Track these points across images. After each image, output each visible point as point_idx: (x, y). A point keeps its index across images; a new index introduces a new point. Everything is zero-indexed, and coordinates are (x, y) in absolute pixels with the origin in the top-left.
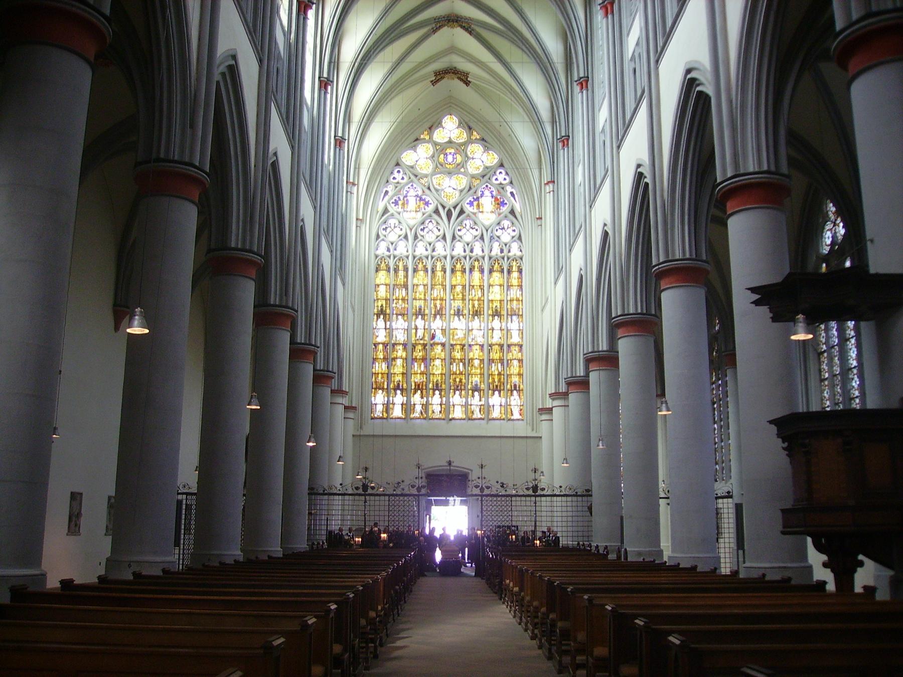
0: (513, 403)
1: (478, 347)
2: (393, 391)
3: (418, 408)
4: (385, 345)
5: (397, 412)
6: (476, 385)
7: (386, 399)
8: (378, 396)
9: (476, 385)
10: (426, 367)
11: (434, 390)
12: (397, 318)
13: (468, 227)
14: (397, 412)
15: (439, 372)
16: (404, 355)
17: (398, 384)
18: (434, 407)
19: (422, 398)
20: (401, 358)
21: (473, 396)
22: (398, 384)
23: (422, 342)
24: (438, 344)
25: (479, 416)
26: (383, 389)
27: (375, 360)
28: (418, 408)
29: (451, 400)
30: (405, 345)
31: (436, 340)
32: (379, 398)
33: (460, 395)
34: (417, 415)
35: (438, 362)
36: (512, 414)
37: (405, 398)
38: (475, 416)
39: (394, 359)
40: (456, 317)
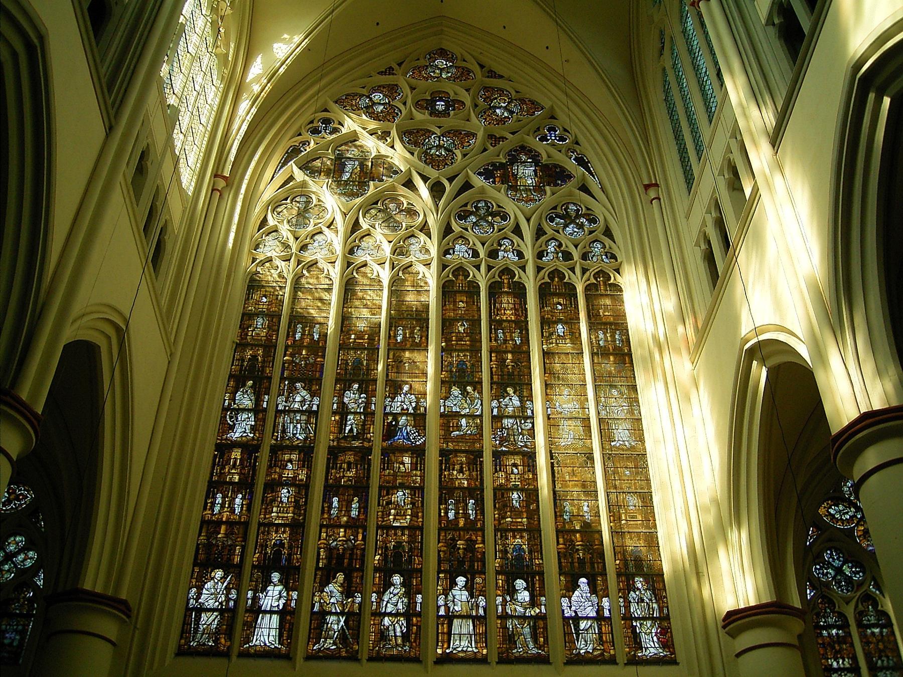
0: (636, 610)
1: (518, 460)
2: (257, 574)
3: (335, 624)
4: (249, 448)
5: (267, 633)
6: (519, 558)
7: (233, 595)
8: (209, 585)
9: (519, 558)
10: (364, 507)
11: (386, 573)
12: (292, 390)
13: (482, 212)
14: (267, 633)
15: (405, 522)
16: (302, 476)
17: (278, 554)
18: (387, 621)
19: (348, 592)
20: (293, 483)
21: (512, 591)
22: (278, 554)
23: (356, 444)
24: (403, 450)
25: (535, 651)
26: (227, 568)
27: (215, 486)
28: (335, 624)
29: (441, 602)
30: (306, 452)
31: (399, 440)
32: (213, 591)
33: (469, 587)
34: (329, 644)
35: (399, 496)
36: (639, 646)
37: (295, 595)
38: (518, 651)
39: (273, 486)
40: (456, 391)
